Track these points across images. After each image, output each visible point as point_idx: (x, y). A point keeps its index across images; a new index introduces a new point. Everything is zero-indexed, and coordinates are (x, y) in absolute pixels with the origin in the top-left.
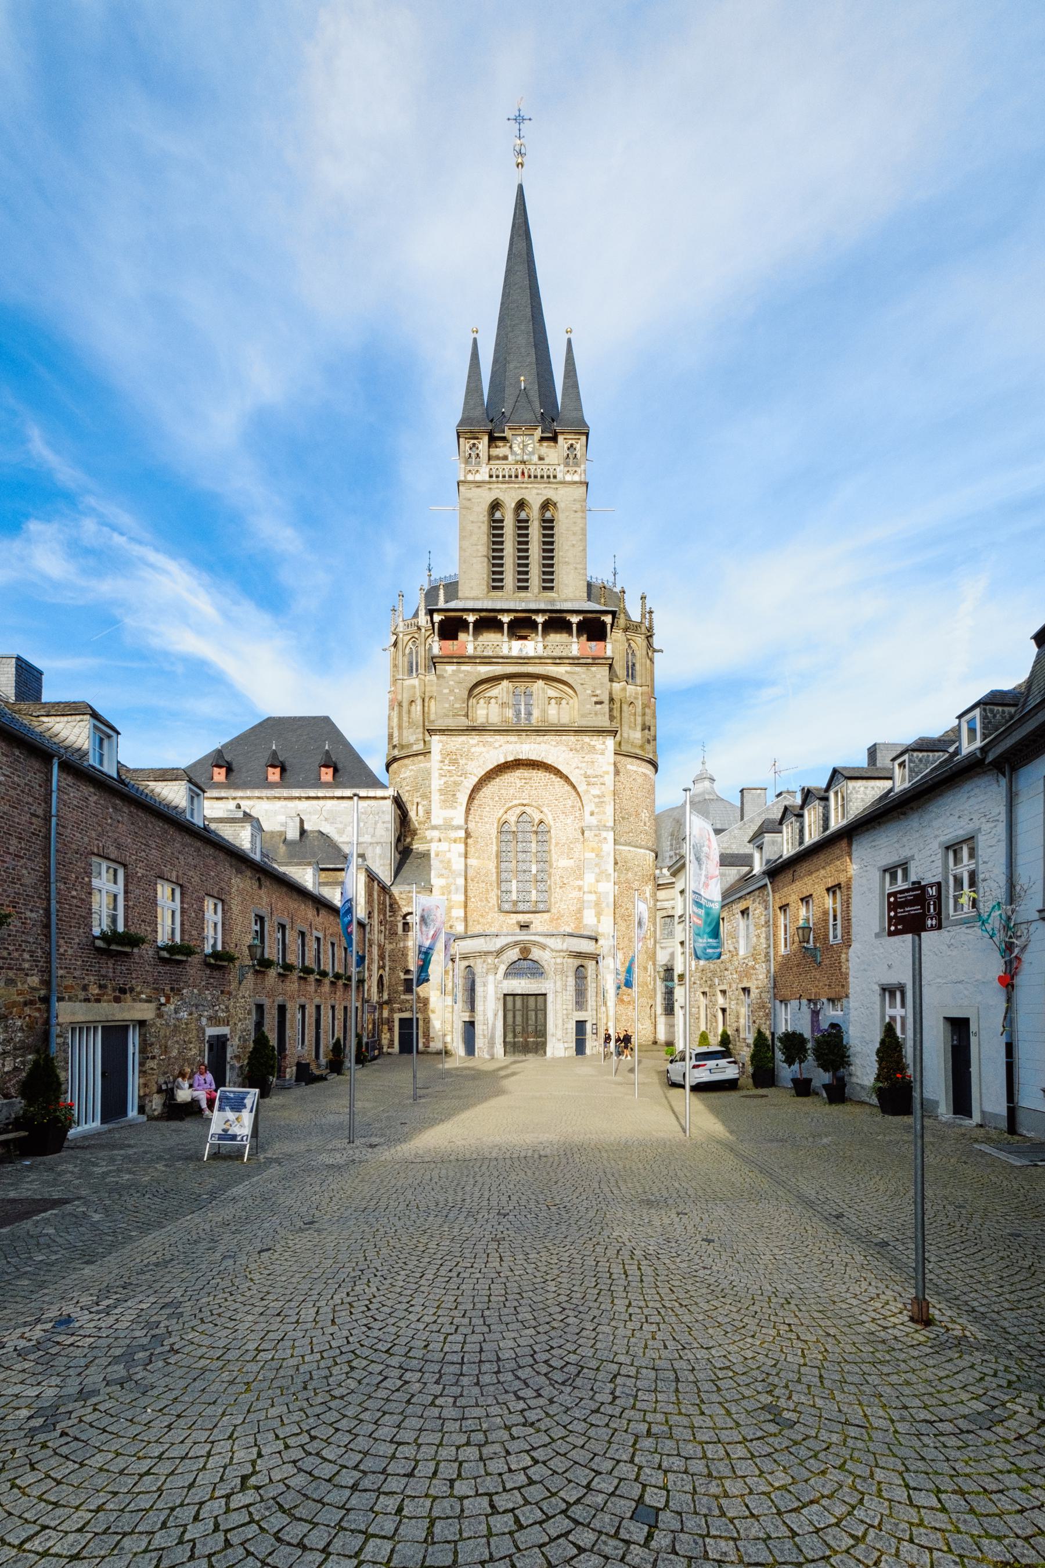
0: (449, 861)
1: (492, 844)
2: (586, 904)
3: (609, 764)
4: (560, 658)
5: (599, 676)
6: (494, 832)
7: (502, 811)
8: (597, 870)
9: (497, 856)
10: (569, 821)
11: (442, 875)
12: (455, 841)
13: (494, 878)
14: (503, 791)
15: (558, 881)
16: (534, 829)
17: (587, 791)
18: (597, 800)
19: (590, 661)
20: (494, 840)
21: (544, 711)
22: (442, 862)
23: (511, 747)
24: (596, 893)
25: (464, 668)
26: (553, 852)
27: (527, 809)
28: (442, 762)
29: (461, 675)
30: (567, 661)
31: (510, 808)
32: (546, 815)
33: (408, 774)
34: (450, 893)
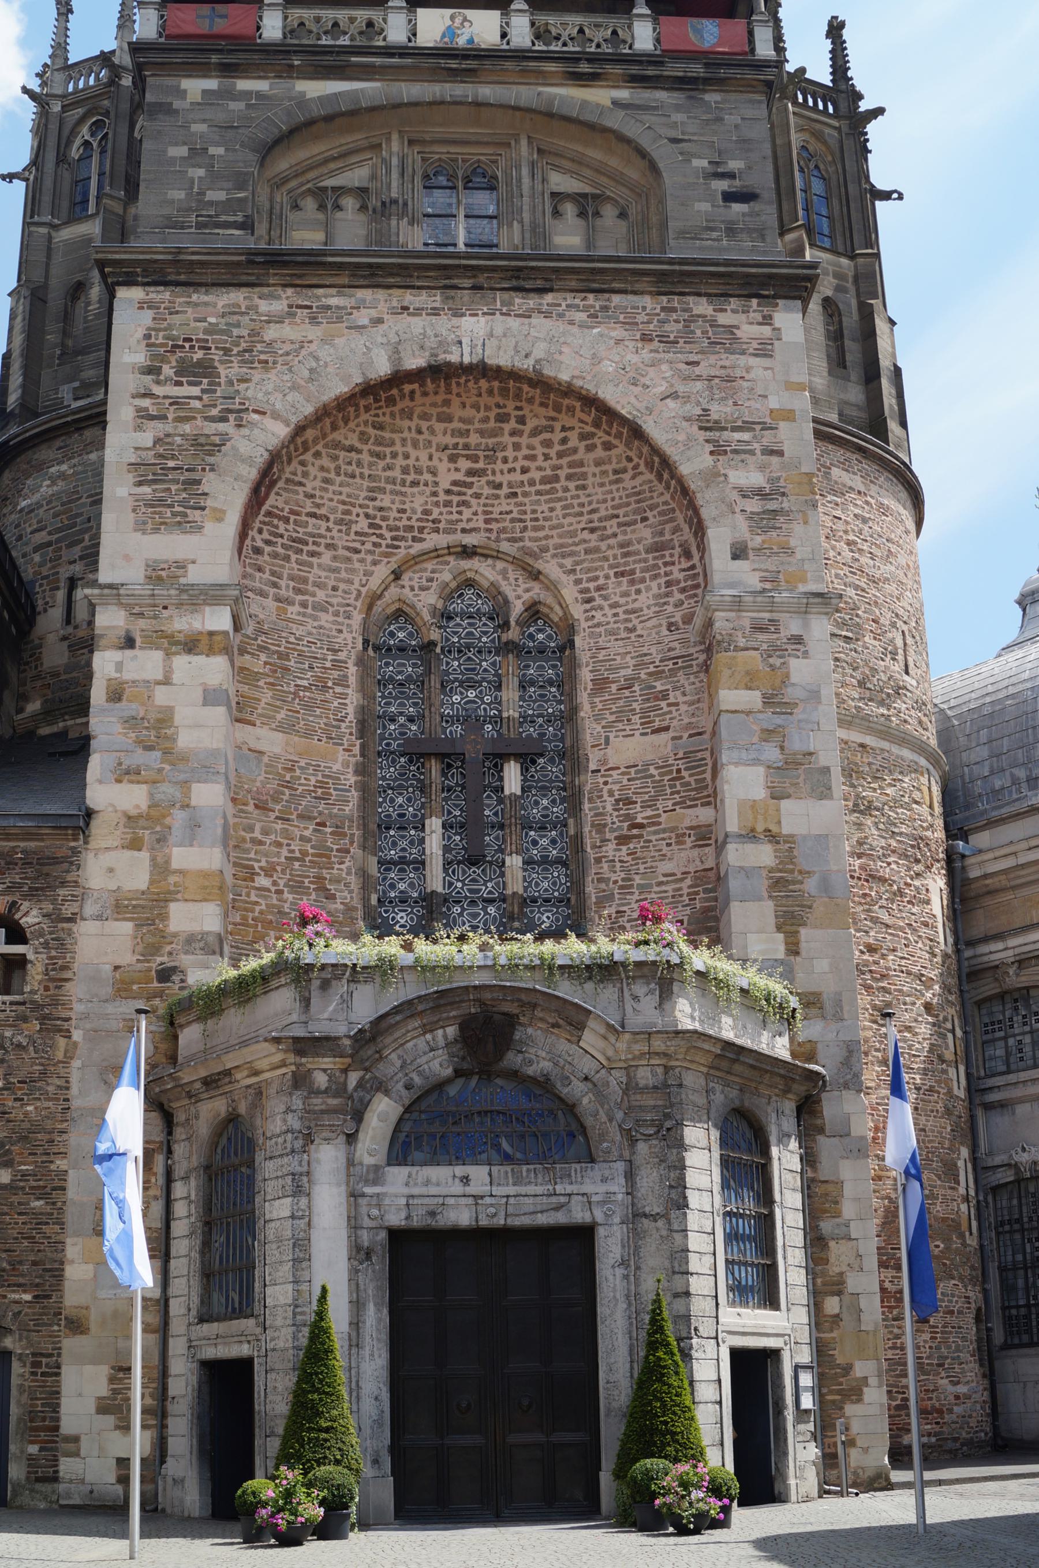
0: (164, 720)
1: (342, 682)
2: (734, 884)
3: (791, 387)
4: (592, 59)
5: (731, 119)
6: (351, 640)
7: (382, 572)
8: (772, 753)
9: (363, 728)
10: (644, 600)
11: (126, 774)
12: (191, 645)
13: (351, 806)
14: (385, 501)
15: (612, 818)
16: (513, 634)
17: (713, 476)
18: (754, 505)
19: (697, 69)
20: (352, 670)
21: (539, 232)
22: (131, 722)
23: (417, 324)
24: (773, 838)
25: (243, 85)
26: (585, 712)
27: (486, 571)
28: (152, 370)
29: (234, 106)
30: (617, 70)
31: (414, 561)
32: (553, 587)
33: (46, 489)
34: (161, 840)
